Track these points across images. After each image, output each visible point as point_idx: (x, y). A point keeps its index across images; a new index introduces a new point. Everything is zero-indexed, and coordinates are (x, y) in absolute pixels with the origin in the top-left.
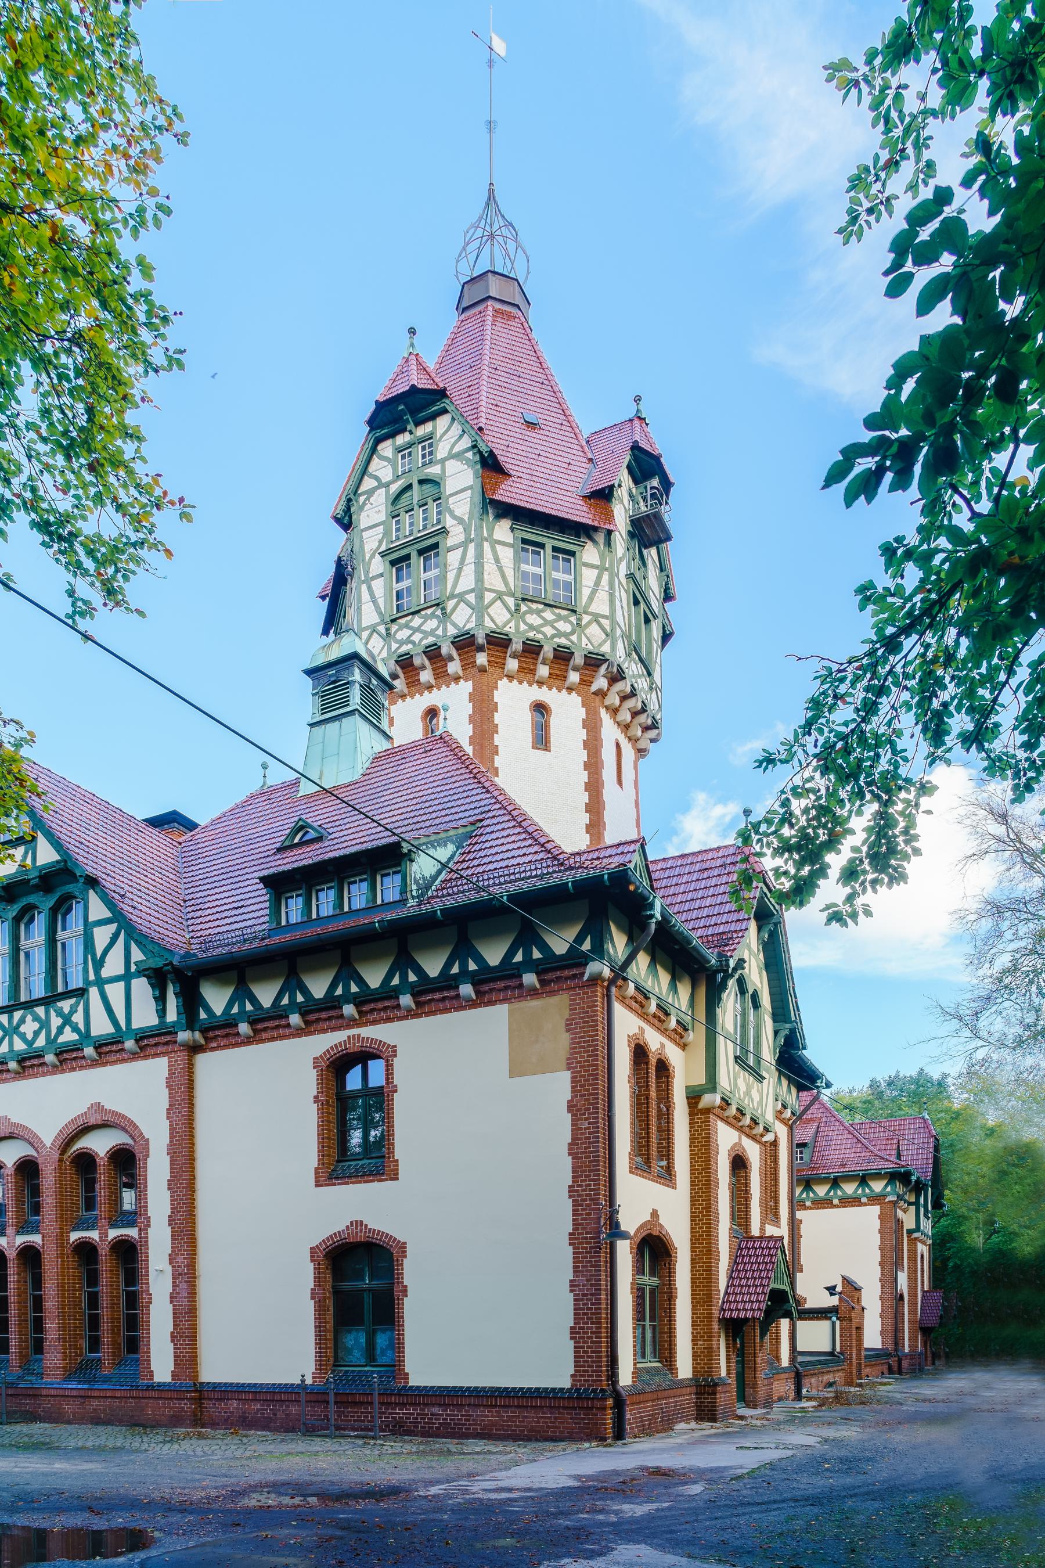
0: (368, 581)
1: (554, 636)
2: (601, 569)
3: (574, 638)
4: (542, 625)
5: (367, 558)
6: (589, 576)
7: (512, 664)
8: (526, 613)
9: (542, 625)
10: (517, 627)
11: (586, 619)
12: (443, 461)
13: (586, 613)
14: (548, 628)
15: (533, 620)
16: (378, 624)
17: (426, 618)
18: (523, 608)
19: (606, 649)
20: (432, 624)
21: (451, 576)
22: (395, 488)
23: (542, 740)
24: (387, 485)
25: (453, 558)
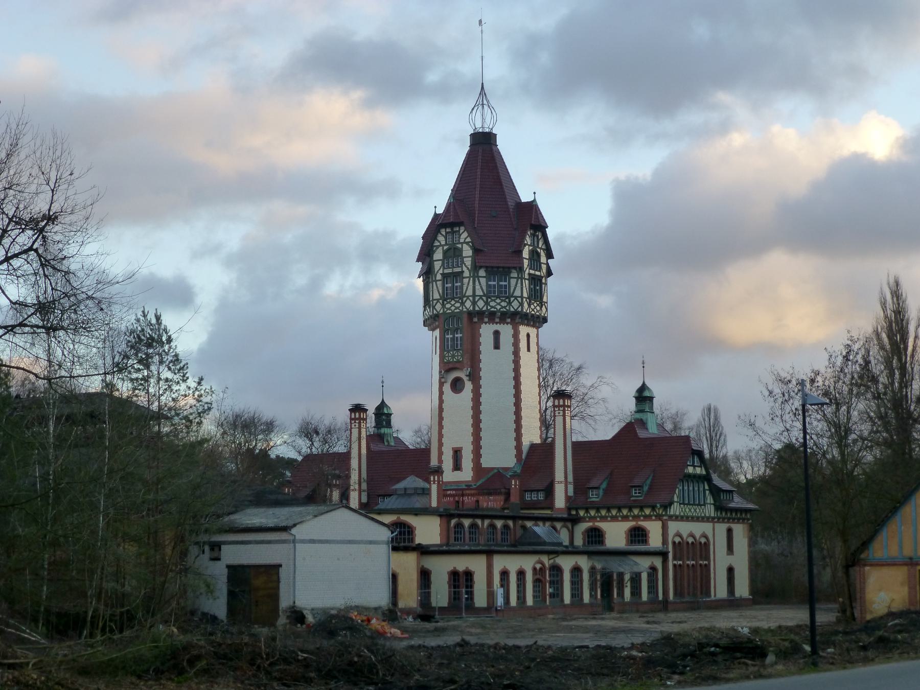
0: (436, 281)
2: (517, 278)
6: (513, 282)
11: (512, 299)
12: (462, 243)
14: (497, 305)
15: (492, 304)
19: (520, 309)
20: (458, 305)
21: (465, 288)
22: (445, 248)
23: (497, 346)
24: (443, 246)
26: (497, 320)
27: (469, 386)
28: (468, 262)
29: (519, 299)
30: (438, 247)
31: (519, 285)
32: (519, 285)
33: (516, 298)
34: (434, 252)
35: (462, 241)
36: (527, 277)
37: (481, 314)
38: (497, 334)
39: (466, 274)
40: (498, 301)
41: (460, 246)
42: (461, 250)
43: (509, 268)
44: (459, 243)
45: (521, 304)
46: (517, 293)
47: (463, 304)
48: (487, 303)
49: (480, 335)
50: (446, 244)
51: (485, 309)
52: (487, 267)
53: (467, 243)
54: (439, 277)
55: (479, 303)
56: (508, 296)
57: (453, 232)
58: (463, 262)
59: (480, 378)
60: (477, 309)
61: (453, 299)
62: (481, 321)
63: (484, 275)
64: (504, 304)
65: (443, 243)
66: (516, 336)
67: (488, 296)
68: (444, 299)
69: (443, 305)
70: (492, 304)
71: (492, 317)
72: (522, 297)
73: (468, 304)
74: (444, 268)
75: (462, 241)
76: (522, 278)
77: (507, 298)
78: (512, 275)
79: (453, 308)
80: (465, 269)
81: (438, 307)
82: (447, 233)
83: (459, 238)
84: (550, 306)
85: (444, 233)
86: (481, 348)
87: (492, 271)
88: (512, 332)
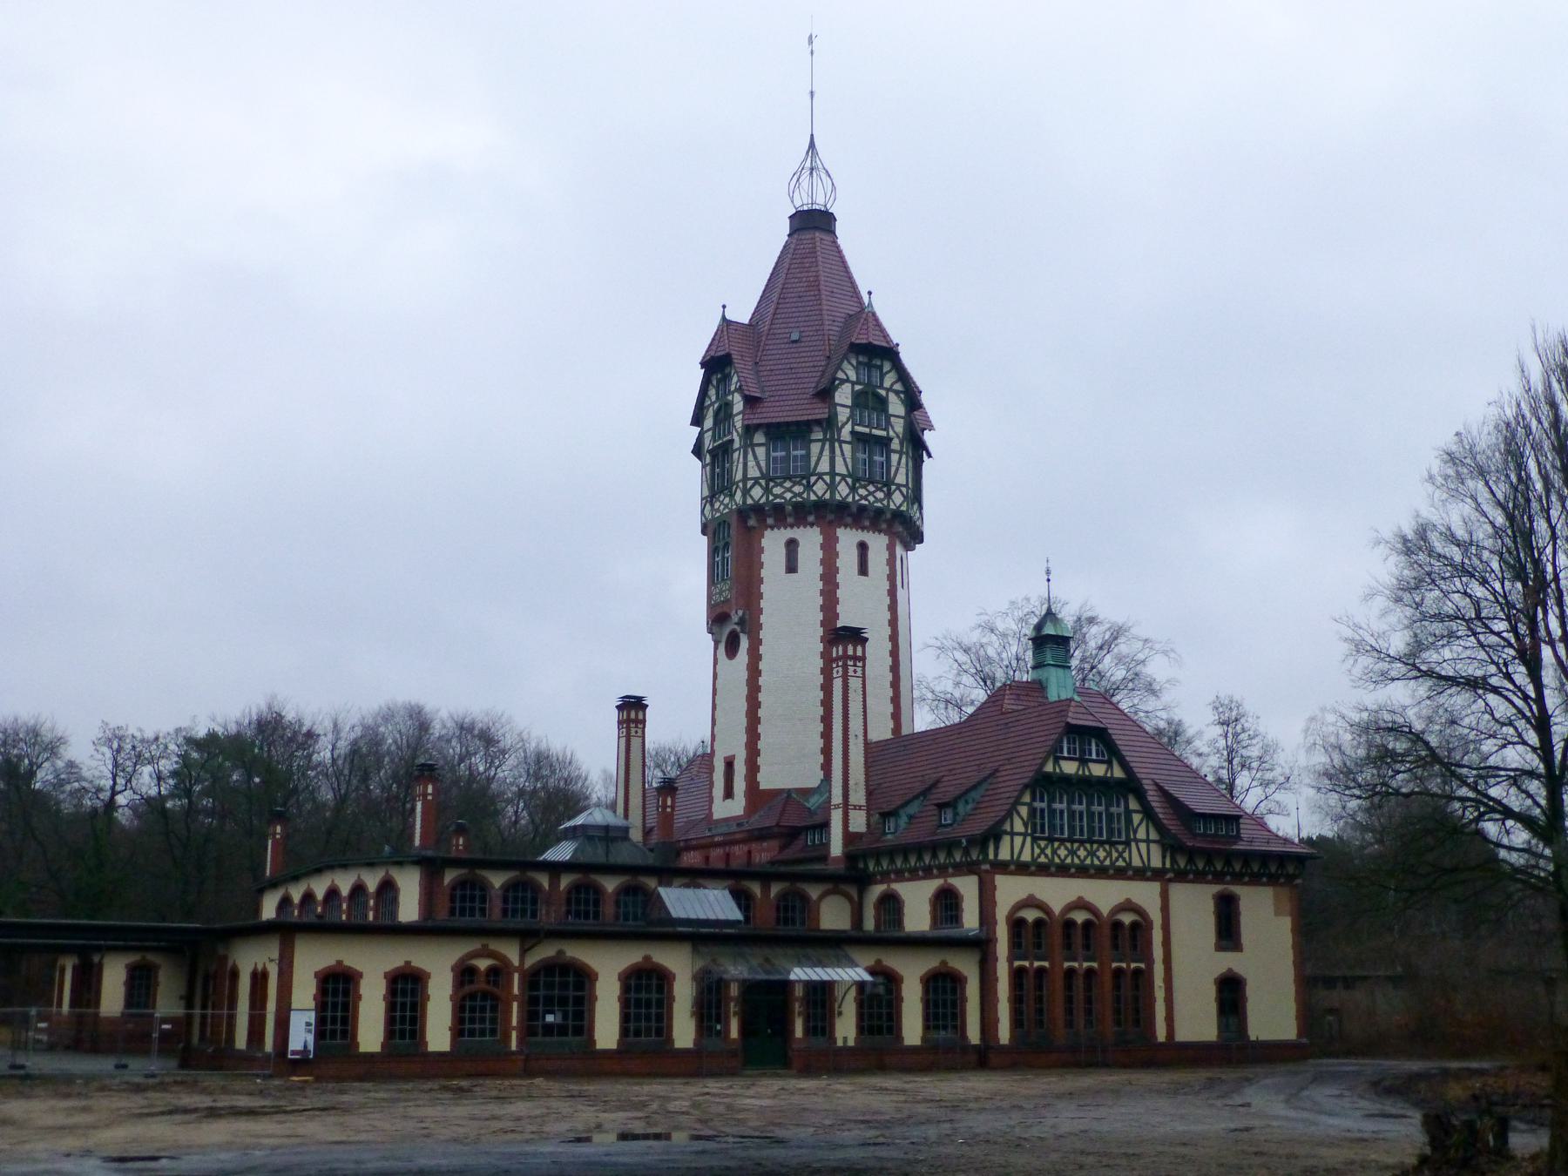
2: (823, 441)
6: (815, 448)
11: (813, 479)
13: (813, 474)
14: (786, 493)
25: (736, 455)
27: (744, 643)
32: (826, 452)
33: (820, 476)
36: (848, 438)
37: (758, 509)
38: (792, 545)
45: (832, 487)
48: (767, 490)
52: (768, 426)
56: (806, 476)
59: (760, 626)
60: (749, 501)
63: (762, 440)
64: (797, 489)
67: (768, 479)
71: (780, 515)
72: (833, 473)
78: (814, 437)
86: (763, 573)
87: (780, 433)
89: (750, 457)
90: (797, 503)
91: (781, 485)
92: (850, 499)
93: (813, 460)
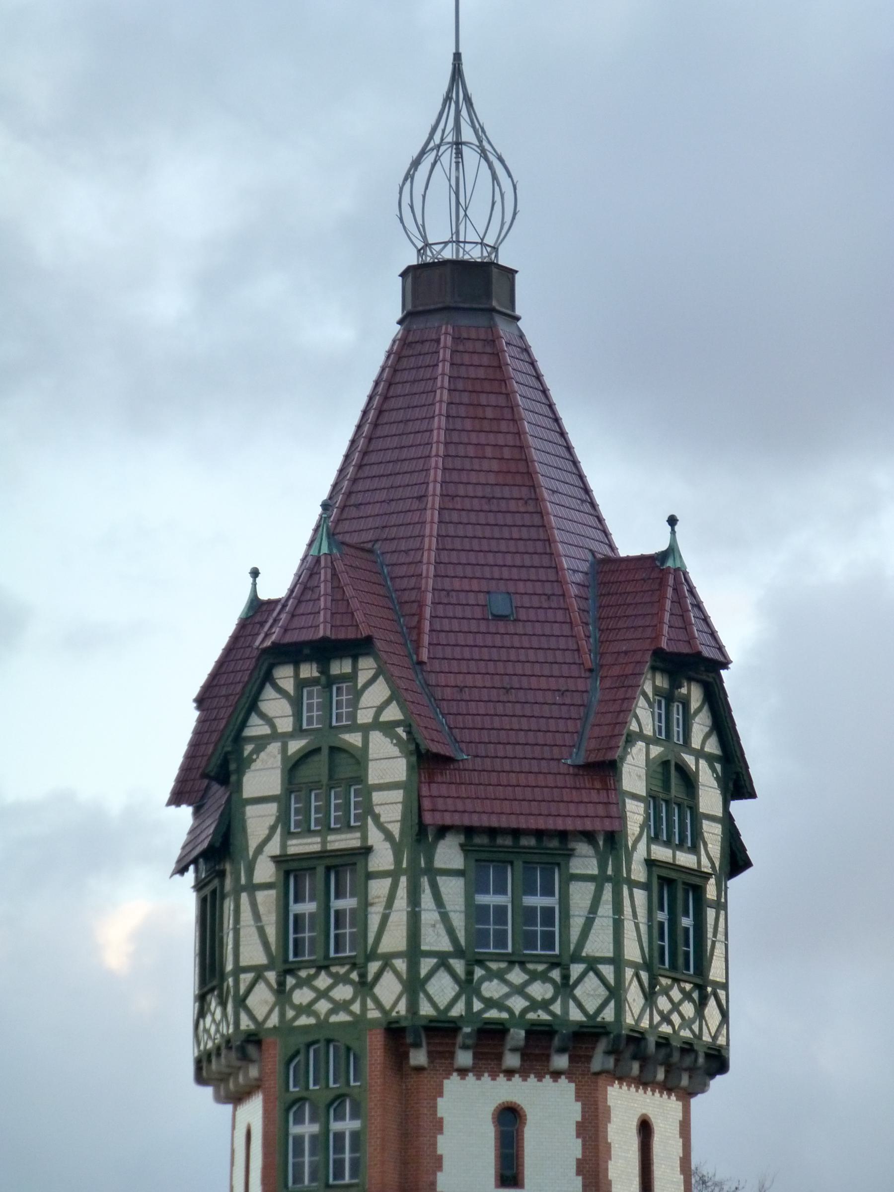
0: (253, 888)
1: (525, 1011)
2: (599, 880)
3: (557, 1008)
4: (507, 996)
5: (251, 853)
7: (464, 1058)
8: (482, 980)
9: (507, 996)
10: (469, 1005)
11: (576, 970)
12: (365, 729)
13: (576, 958)
14: (515, 995)
15: (492, 989)
16: (266, 968)
17: (338, 980)
18: (479, 972)
20: (343, 992)
22: (295, 746)
24: (284, 738)
25: (379, 888)
26: (512, 1060)
28: (390, 808)
29: (608, 971)
30: (261, 742)
31: (606, 909)
32: (606, 909)
33: (592, 964)
34: (244, 764)
35: (364, 717)
36: (639, 873)
38: (509, 1118)
39: (383, 858)
40: (517, 976)
41: (354, 739)
42: (359, 759)
43: (563, 835)
44: (354, 727)
45: (616, 993)
46: (599, 944)
47: (365, 987)
48: (467, 986)
49: (438, 1126)
50: (298, 731)
51: (458, 1010)
52: (469, 831)
53: (388, 728)
54: (265, 871)
55: (432, 987)
57: (329, 682)
58: (368, 810)
60: (426, 1009)
61: (323, 966)
62: (443, 1059)
64: (540, 991)
65: (285, 725)
66: (592, 1128)
68: (286, 966)
69: (281, 993)
70: (492, 989)
71: (489, 1042)
72: (617, 961)
73: (389, 990)
74: (288, 834)
75: (364, 717)
76: (619, 881)
77: (554, 964)
78: (577, 866)
79: (323, 1006)
80: (375, 837)
81: (261, 1000)
82: (301, 684)
83: (354, 703)
84: (740, 999)
85: (288, 685)
87: (495, 849)
88: (575, 1111)
89: (427, 899)
90: (534, 1023)
91: (500, 976)
92: (645, 1024)
93: (576, 924)
